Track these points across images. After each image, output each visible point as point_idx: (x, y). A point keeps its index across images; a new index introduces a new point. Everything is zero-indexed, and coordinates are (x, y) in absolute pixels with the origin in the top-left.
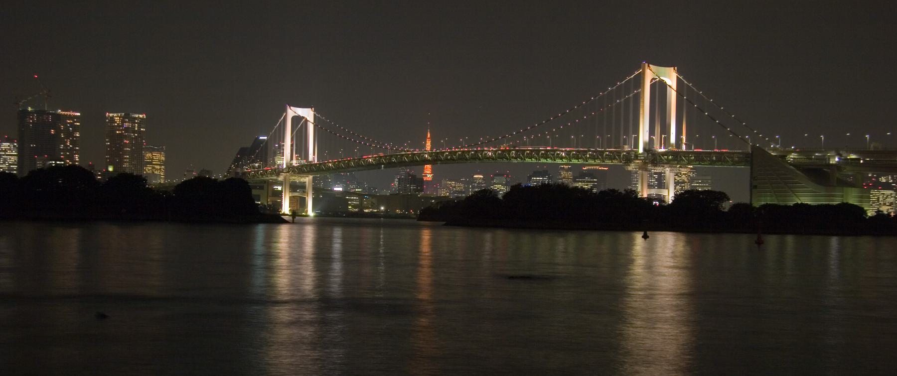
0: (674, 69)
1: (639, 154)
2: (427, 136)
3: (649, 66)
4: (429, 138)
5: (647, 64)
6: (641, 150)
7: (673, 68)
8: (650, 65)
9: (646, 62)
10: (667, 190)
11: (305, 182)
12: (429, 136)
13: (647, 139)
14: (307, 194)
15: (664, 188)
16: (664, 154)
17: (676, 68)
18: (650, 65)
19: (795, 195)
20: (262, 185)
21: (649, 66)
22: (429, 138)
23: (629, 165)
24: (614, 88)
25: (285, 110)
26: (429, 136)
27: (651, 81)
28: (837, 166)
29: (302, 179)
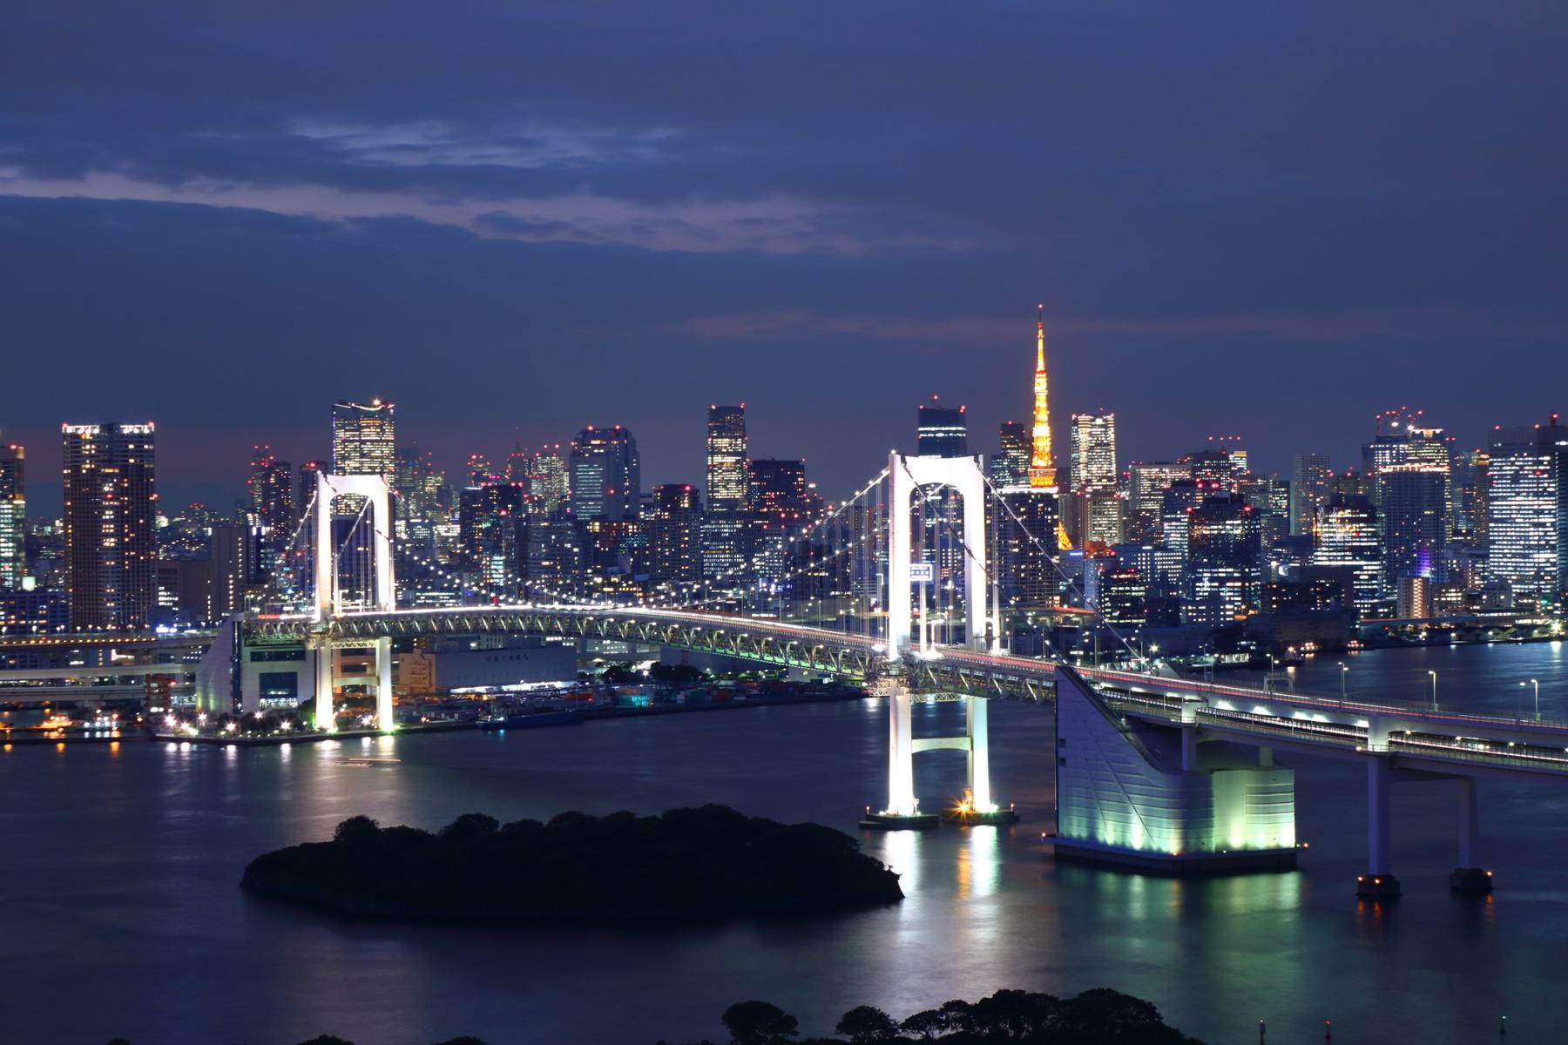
0: (976, 460)
1: (894, 663)
3: (903, 461)
4: (1042, 372)
5: (898, 458)
6: (894, 656)
7: (972, 458)
8: (908, 458)
9: (897, 453)
10: (968, 739)
11: (374, 649)
12: (1041, 365)
13: (907, 631)
15: (964, 734)
16: (936, 666)
17: (981, 457)
18: (907, 458)
19: (1122, 786)
20: (298, 648)
21: (903, 461)
22: (1042, 372)
24: (852, 502)
25: (310, 484)
26: (1041, 365)
27: (914, 496)
28: (1195, 729)
29: (367, 642)
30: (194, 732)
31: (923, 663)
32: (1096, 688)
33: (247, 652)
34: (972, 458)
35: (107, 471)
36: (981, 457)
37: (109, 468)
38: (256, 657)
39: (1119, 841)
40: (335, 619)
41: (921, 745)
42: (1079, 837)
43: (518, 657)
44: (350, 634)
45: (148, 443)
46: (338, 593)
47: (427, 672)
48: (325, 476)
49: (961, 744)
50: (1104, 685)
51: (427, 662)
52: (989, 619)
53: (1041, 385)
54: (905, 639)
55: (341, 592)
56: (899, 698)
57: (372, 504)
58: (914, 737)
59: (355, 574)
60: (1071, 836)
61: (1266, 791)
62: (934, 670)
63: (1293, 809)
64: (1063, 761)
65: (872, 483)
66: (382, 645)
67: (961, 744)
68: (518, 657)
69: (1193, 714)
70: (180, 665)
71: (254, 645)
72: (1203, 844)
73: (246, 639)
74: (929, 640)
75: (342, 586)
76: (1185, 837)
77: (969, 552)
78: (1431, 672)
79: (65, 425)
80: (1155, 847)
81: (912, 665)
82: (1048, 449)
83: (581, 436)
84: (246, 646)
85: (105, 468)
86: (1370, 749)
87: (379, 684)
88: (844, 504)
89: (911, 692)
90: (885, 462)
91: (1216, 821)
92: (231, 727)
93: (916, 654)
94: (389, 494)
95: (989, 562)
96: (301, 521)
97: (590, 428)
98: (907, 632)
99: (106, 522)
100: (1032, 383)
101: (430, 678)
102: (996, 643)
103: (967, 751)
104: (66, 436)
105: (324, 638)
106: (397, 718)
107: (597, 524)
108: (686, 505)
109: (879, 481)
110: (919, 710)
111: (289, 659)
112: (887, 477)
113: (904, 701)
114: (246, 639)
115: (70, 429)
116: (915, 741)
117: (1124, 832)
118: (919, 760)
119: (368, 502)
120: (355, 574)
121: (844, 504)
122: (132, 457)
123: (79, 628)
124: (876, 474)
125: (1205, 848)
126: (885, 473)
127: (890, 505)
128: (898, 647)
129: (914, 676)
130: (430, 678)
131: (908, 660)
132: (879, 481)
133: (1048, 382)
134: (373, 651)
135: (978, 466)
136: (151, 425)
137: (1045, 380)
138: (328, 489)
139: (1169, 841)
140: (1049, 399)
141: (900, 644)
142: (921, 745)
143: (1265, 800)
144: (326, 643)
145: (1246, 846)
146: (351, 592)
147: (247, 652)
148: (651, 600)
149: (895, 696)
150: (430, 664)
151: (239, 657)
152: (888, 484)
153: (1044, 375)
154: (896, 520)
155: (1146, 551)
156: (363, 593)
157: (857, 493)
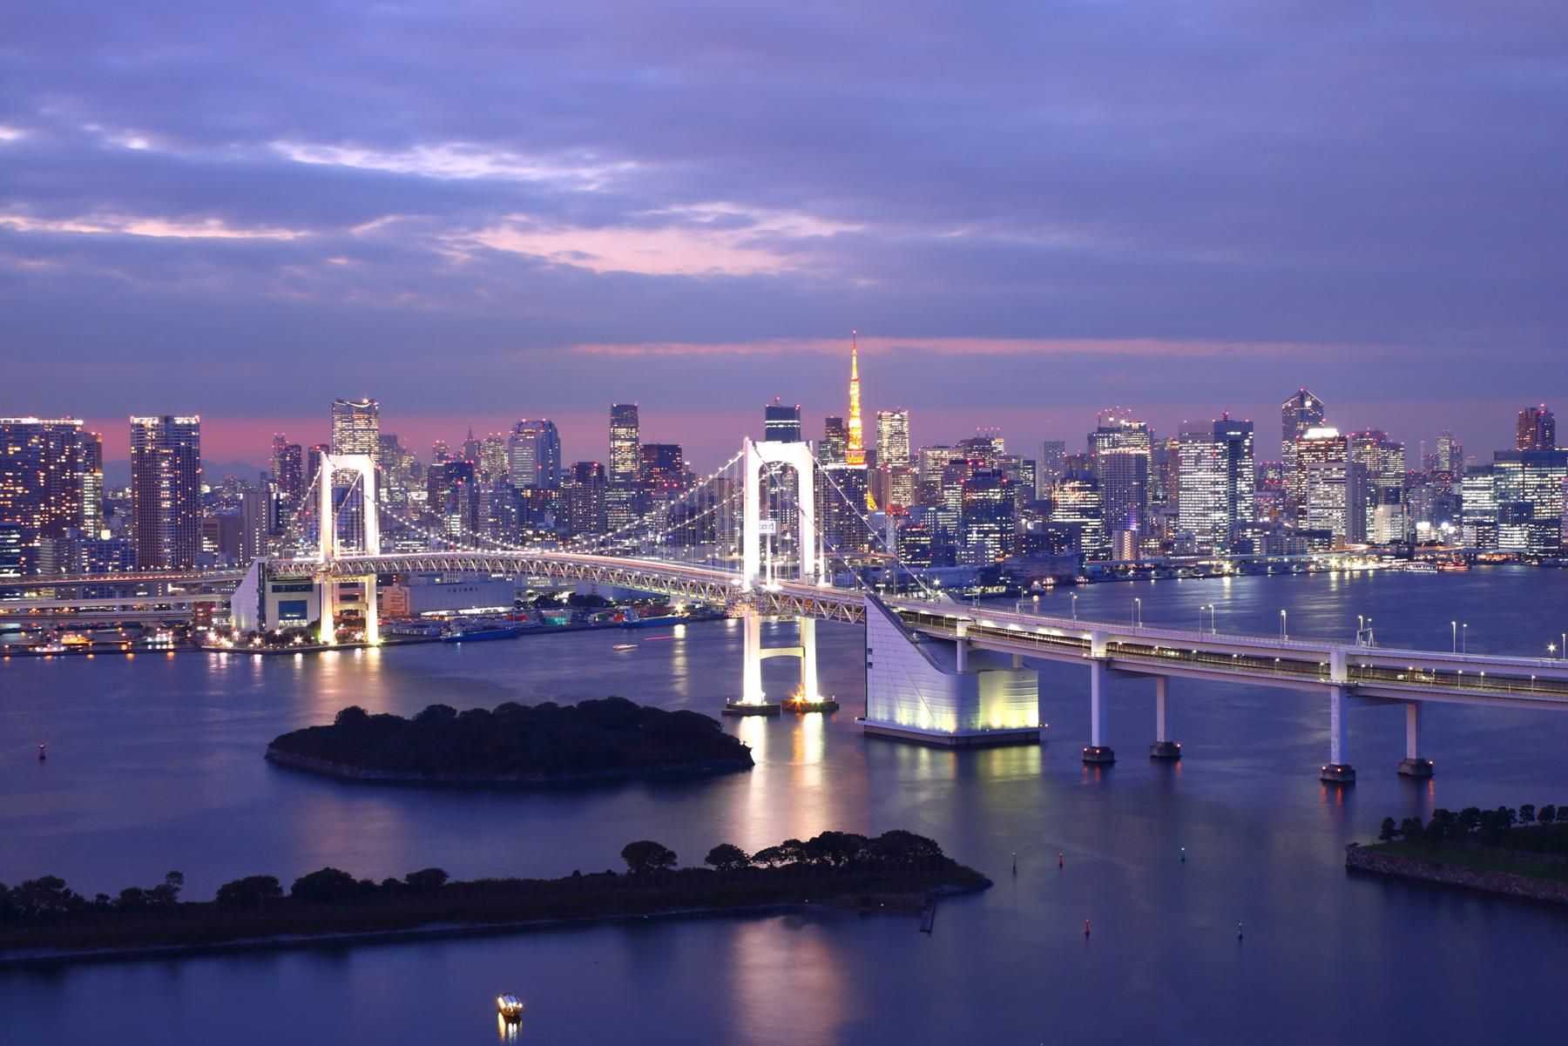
0: (808, 445)
2: (851, 375)
4: (855, 380)
5: (751, 442)
6: (747, 588)
7: (805, 443)
8: (757, 443)
9: (750, 439)
10: (801, 649)
11: (364, 583)
12: (855, 375)
14: (367, 605)
17: (811, 443)
18: (757, 443)
20: (308, 583)
21: (754, 444)
22: (855, 380)
23: (734, 609)
25: (315, 462)
26: (855, 375)
27: (762, 471)
29: (359, 578)
30: (230, 645)
31: (767, 594)
32: (895, 611)
33: (269, 585)
34: (805, 443)
35: (164, 451)
36: (811, 443)
37: (166, 449)
38: (276, 589)
39: (911, 723)
40: (335, 561)
41: (768, 653)
42: (882, 720)
43: (471, 589)
44: (345, 572)
45: (194, 431)
46: (337, 542)
47: (403, 600)
48: (327, 456)
49: (797, 652)
50: (900, 609)
51: (403, 593)
52: (817, 561)
53: (855, 390)
54: (755, 575)
55: (339, 541)
56: (751, 618)
57: (362, 476)
58: (761, 648)
59: (350, 530)
60: (877, 719)
61: (1018, 686)
62: (776, 597)
63: (1037, 699)
64: (871, 664)
65: (731, 462)
66: (369, 581)
67: (797, 652)
68: (471, 589)
69: (965, 630)
70: (219, 595)
71: (275, 580)
74: (773, 577)
75: (340, 538)
76: (959, 720)
77: (802, 511)
78: (1137, 600)
79: (132, 417)
80: (937, 727)
81: (760, 595)
82: (860, 437)
83: (516, 427)
85: (162, 448)
86: (1093, 655)
87: (368, 609)
88: (711, 476)
89: (760, 614)
90: (741, 446)
91: (981, 708)
92: (258, 641)
93: (763, 586)
94: (375, 469)
95: (817, 519)
96: (310, 488)
97: (524, 421)
98: (757, 571)
99: (164, 489)
100: (848, 388)
101: (406, 605)
102: (822, 579)
103: (800, 658)
104: (133, 426)
106: (381, 634)
107: (529, 491)
108: (595, 474)
109: (736, 460)
110: (765, 626)
111: (299, 591)
112: (742, 457)
113: (754, 621)
115: (136, 421)
116: (762, 650)
117: (914, 716)
118: (766, 665)
119: (360, 474)
120: (350, 530)
121: (711, 476)
122: (183, 441)
123: (143, 568)
124: (734, 455)
125: (973, 727)
126: (740, 454)
127: (745, 477)
128: (751, 582)
129: (762, 601)
130: (406, 605)
131: (759, 592)
132: (736, 460)
133: (860, 387)
134: (364, 584)
136: (197, 417)
138: (329, 465)
139: (945, 722)
140: (861, 400)
141: (752, 579)
142: (768, 653)
143: (1017, 691)
144: (328, 579)
145: (1003, 726)
146: (347, 541)
147: (269, 585)
148: (569, 547)
149: (748, 616)
150: (406, 594)
151: (264, 589)
152: (742, 462)
153: (857, 383)
154: (749, 487)
155: (931, 512)
156: (355, 542)
157: (721, 469)
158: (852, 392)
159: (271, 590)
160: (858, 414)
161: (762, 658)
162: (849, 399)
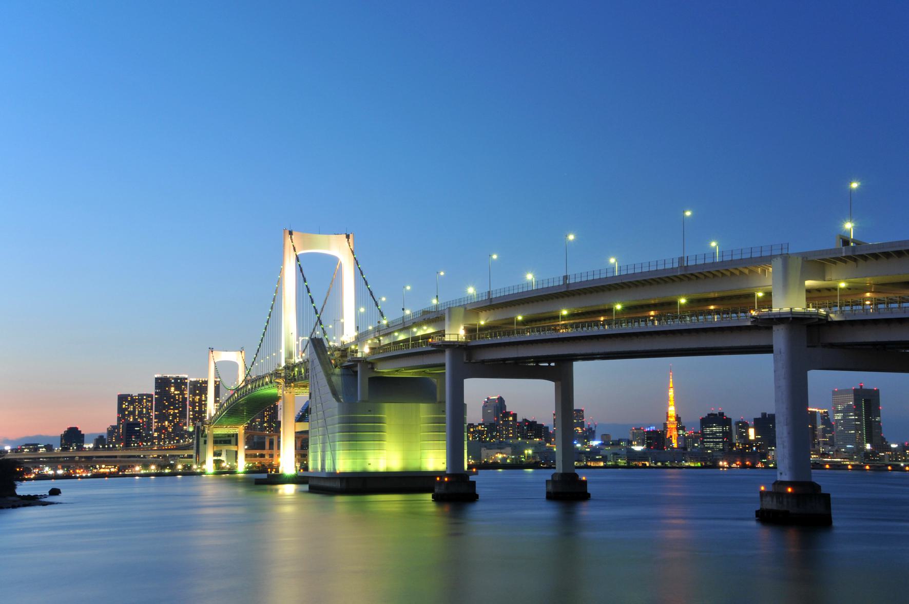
0: (348, 237)
12: (671, 385)
20: (229, 438)
26: (671, 385)
53: (671, 393)
72: (370, 464)
73: (202, 434)
82: (674, 415)
84: (202, 437)
95: (362, 310)
105: (209, 427)
114: (202, 434)
125: (372, 468)
128: (285, 358)
135: (348, 240)
137: (673, 391)
140: (675, 397)
144: (210, 429)
158: (670, 394)
159: (203, 443)
160: (673, 404)
161: (296, 431)
162: (668, 397)
